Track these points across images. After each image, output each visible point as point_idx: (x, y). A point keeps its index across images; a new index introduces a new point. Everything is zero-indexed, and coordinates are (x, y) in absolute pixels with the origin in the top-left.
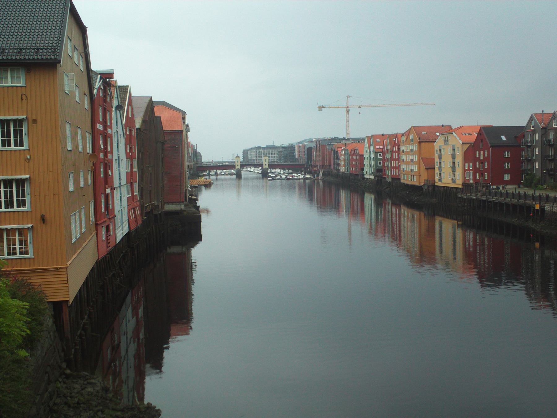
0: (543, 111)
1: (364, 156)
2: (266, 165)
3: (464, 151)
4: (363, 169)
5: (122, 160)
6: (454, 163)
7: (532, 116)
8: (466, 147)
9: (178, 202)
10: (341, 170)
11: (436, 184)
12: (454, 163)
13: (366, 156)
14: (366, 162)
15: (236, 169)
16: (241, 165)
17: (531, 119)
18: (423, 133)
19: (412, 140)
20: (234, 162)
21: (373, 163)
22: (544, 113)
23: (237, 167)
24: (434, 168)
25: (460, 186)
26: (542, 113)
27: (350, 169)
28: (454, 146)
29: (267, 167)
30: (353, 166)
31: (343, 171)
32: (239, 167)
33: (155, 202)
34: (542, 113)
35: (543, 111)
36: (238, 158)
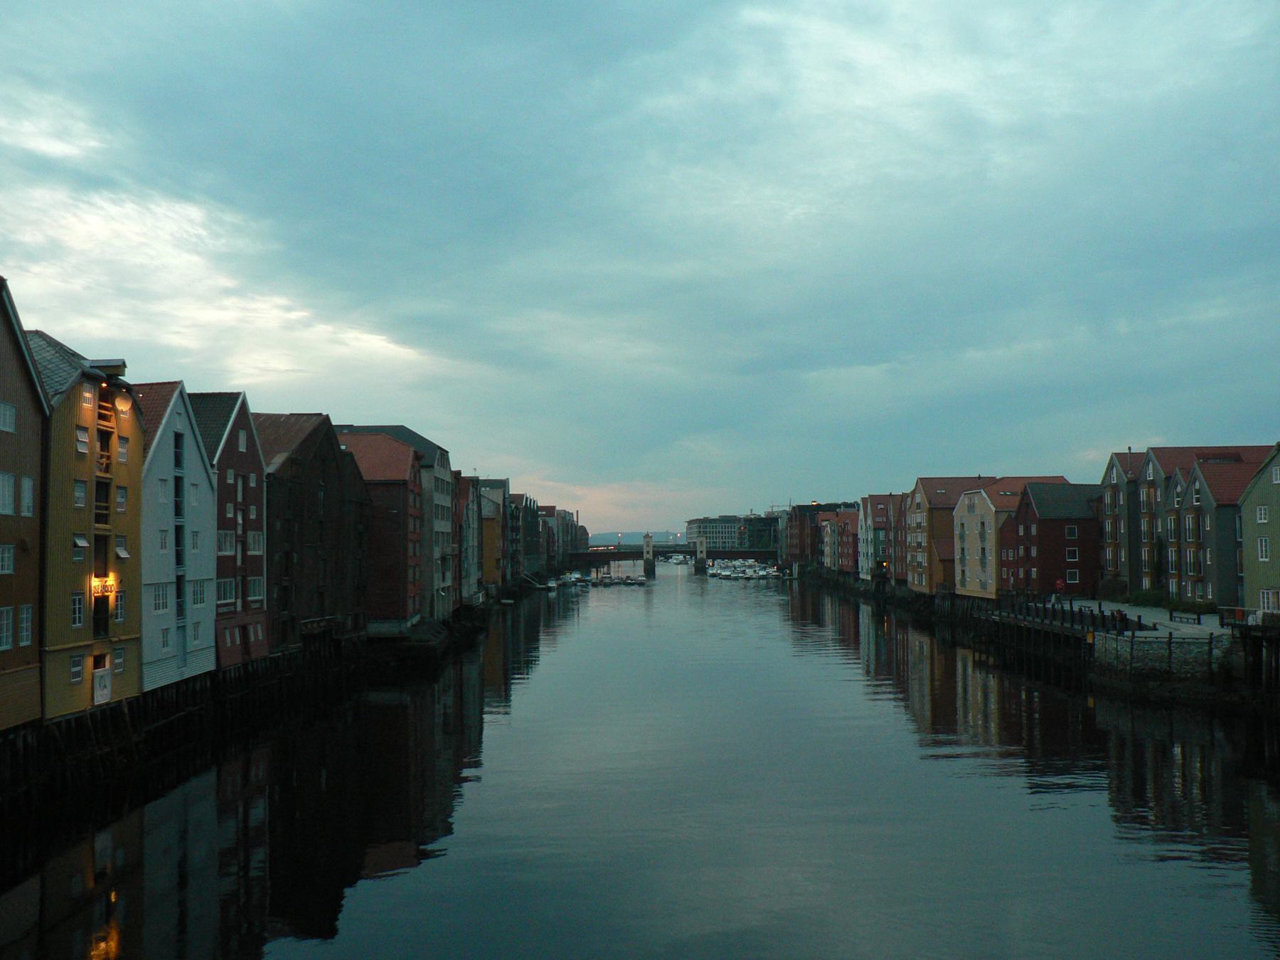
0: (1130, 448)
1: (859, 537)
2: (701, 552)
3: (1000, 526)
4: (856, 562)
5: (195, 533)
6: (983, 549)
7: (1112, 458)
8: (1003, 517)
10: (826, 565)
11: (959, 590)
12: (983, 549)
13: (861, 536)
14: (862, 548)
15: (645, 558)
16: (654, 552)
17: (1111, 466)
18: (938, 491)
19: (919, 506)
20: (641, 547)
21: (871, 550)
22: (1132, 452)
23: (645, 556)
24: (953, 561)
25: (994, 597)
26: (1127, 451)
27: (839, 561)
28: (982, 516)
29: (704, 555)
30: (841, 556)
31: (829, 565)
32: (650, 556)
33: (339, 617)
34: (1127, 451)
35: (1130, 448)
36: (648, 539)
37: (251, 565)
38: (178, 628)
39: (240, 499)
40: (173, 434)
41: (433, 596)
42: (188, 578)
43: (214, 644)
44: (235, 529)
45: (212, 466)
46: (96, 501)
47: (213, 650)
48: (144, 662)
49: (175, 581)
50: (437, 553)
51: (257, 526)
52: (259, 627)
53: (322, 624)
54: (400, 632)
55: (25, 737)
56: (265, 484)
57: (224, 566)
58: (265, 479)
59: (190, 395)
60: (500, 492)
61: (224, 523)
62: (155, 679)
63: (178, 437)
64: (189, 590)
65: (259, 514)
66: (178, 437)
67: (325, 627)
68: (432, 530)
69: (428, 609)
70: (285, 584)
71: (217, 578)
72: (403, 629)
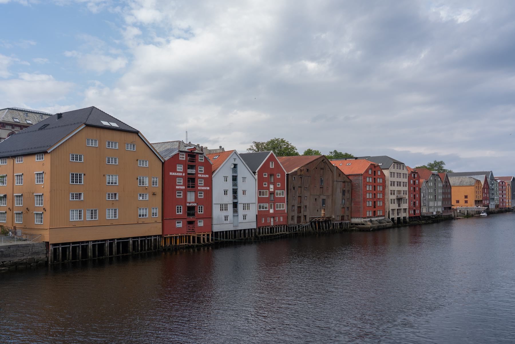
9: (359, 218)
37: (281, 200)
38: (233, 216)
39: (272, 180)
40: (237, 163)
41: (389, 211)
42: (239, 202)
43: (256, 221)
44: (269, 190)
45: (254, 173)
46: (188, 183)
47: (256, 223)
48: (213, 224)
49: (232, 203)
50: (394, 197)
51: (282, 188)
52: (282, 218)
53: (325, 218)
54: (361, 222)
55: (155, 240)
56: (286, 177)
57: (260, 200)
58: (286, 175)
59: (240, 154)
60: (485, 175)
61: (260, 187)
62: (216, 228)
63: (235, 166)
64: (240, 207)
65: (283, 185)
66: (235, 166)
67: (325, 219)
68: (388, 190)
69: (388, 215)
70: (299, 206)
71: (258, 203)
72: (362, 221)
